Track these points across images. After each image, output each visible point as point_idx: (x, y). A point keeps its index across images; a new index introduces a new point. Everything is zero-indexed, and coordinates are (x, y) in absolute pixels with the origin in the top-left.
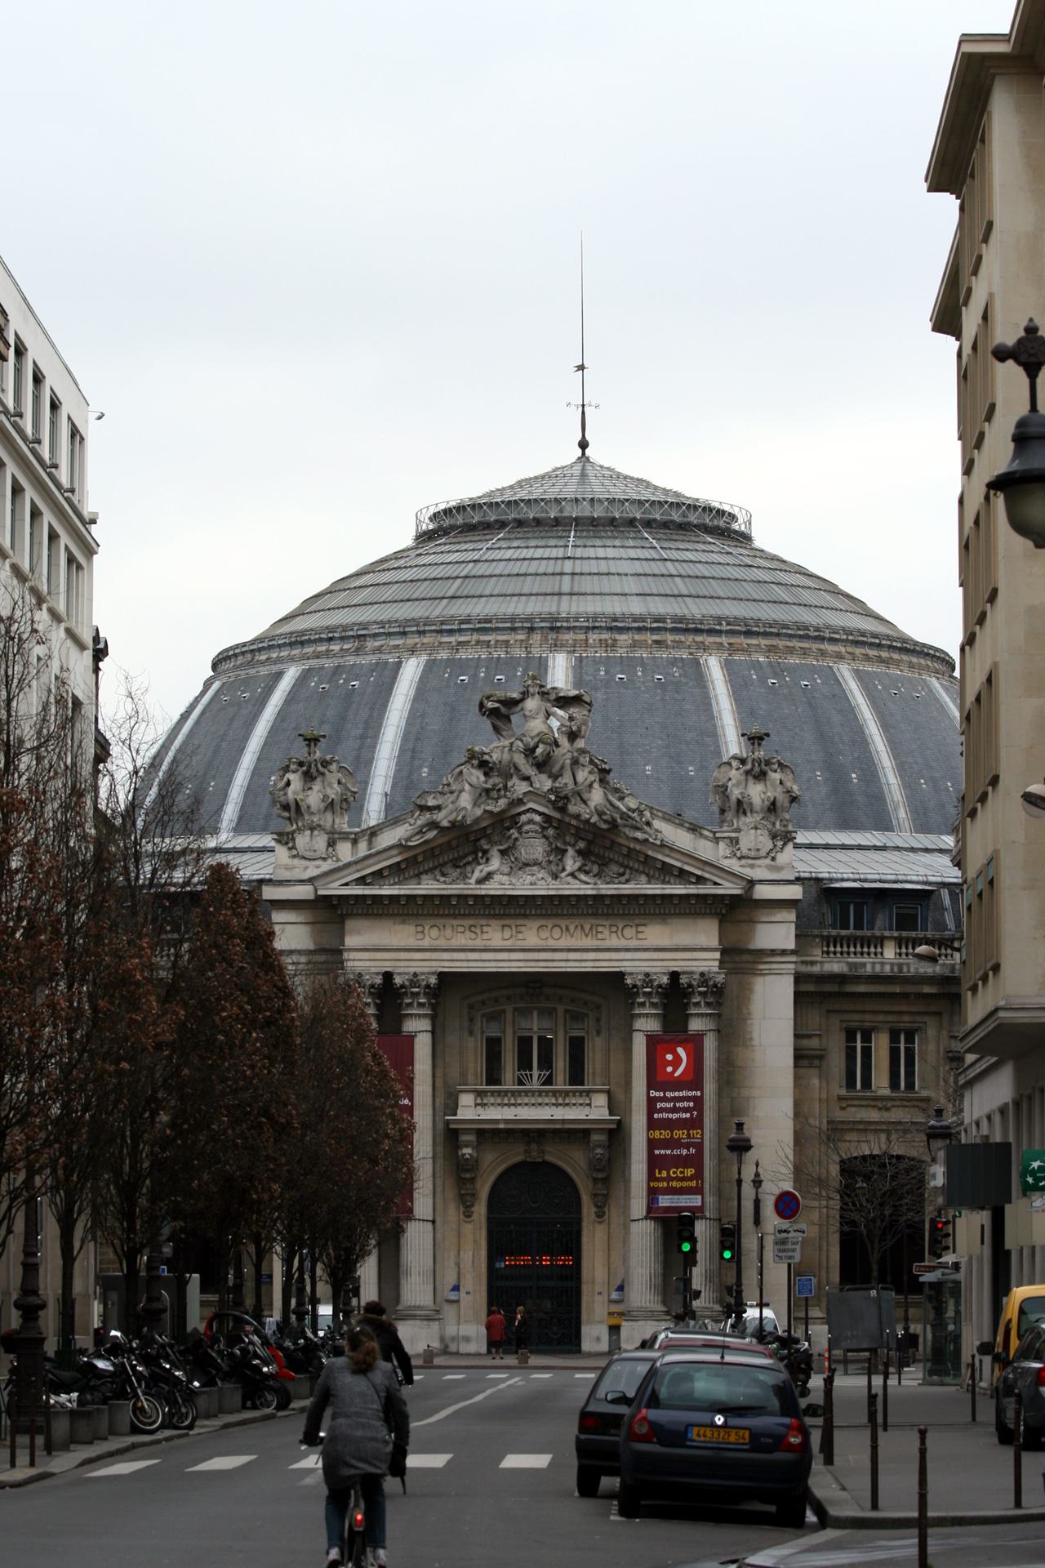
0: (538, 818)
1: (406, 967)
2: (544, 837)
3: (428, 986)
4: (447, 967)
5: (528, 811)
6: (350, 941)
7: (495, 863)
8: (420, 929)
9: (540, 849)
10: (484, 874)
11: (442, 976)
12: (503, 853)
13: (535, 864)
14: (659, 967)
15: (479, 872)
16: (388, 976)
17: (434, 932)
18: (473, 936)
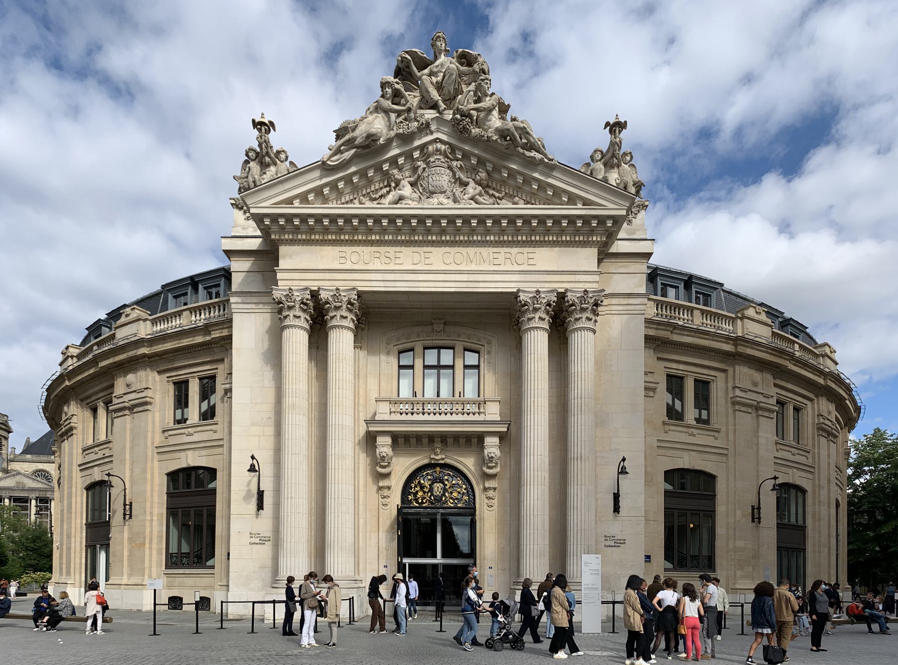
0: (443, 147)
1: (327, 286)
2: (450, 168)
3: (350, 303)
4: (364, 287)
5: (435, 141)
6: (283, 264)
7: (407, 190)
8: (343, 254)
9: (446, 178)
10: (397, 197)
11: (360, 294)
12: (412, 184)
13: (441, 193)
14: (550, 286)
15: (390, 197)
16: (315, 295)
17: (355, 258)
18: (388, 261)
